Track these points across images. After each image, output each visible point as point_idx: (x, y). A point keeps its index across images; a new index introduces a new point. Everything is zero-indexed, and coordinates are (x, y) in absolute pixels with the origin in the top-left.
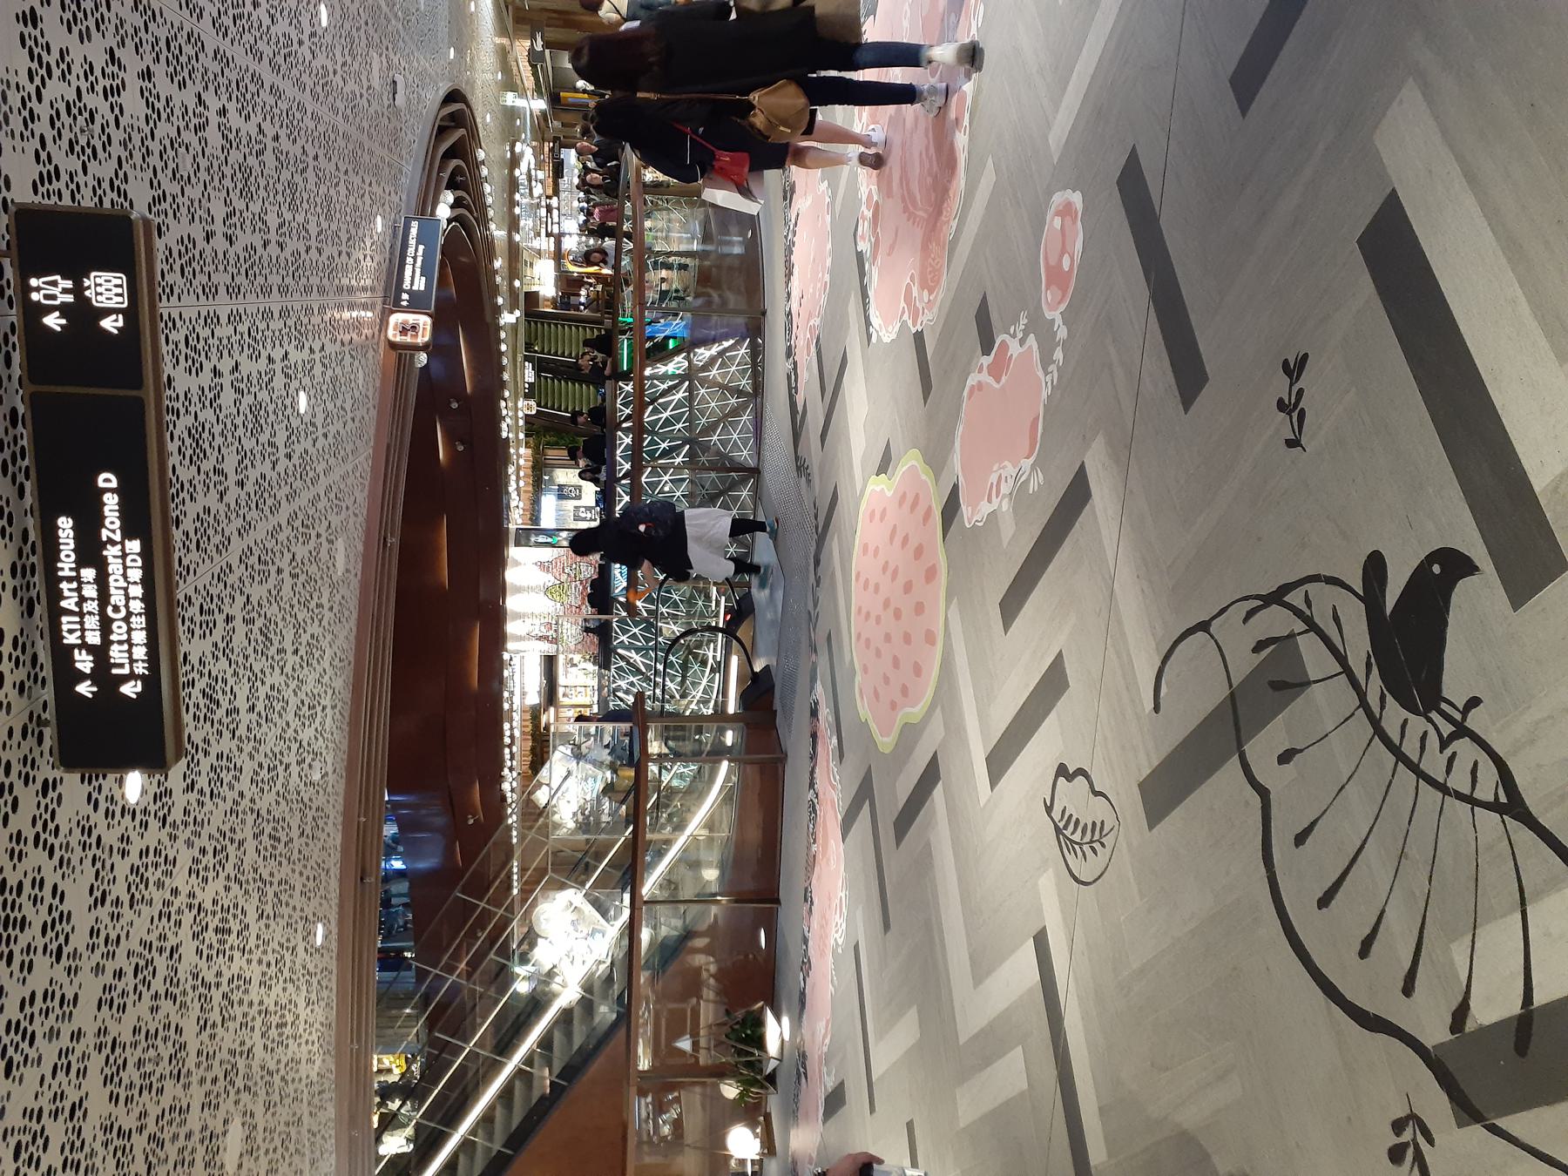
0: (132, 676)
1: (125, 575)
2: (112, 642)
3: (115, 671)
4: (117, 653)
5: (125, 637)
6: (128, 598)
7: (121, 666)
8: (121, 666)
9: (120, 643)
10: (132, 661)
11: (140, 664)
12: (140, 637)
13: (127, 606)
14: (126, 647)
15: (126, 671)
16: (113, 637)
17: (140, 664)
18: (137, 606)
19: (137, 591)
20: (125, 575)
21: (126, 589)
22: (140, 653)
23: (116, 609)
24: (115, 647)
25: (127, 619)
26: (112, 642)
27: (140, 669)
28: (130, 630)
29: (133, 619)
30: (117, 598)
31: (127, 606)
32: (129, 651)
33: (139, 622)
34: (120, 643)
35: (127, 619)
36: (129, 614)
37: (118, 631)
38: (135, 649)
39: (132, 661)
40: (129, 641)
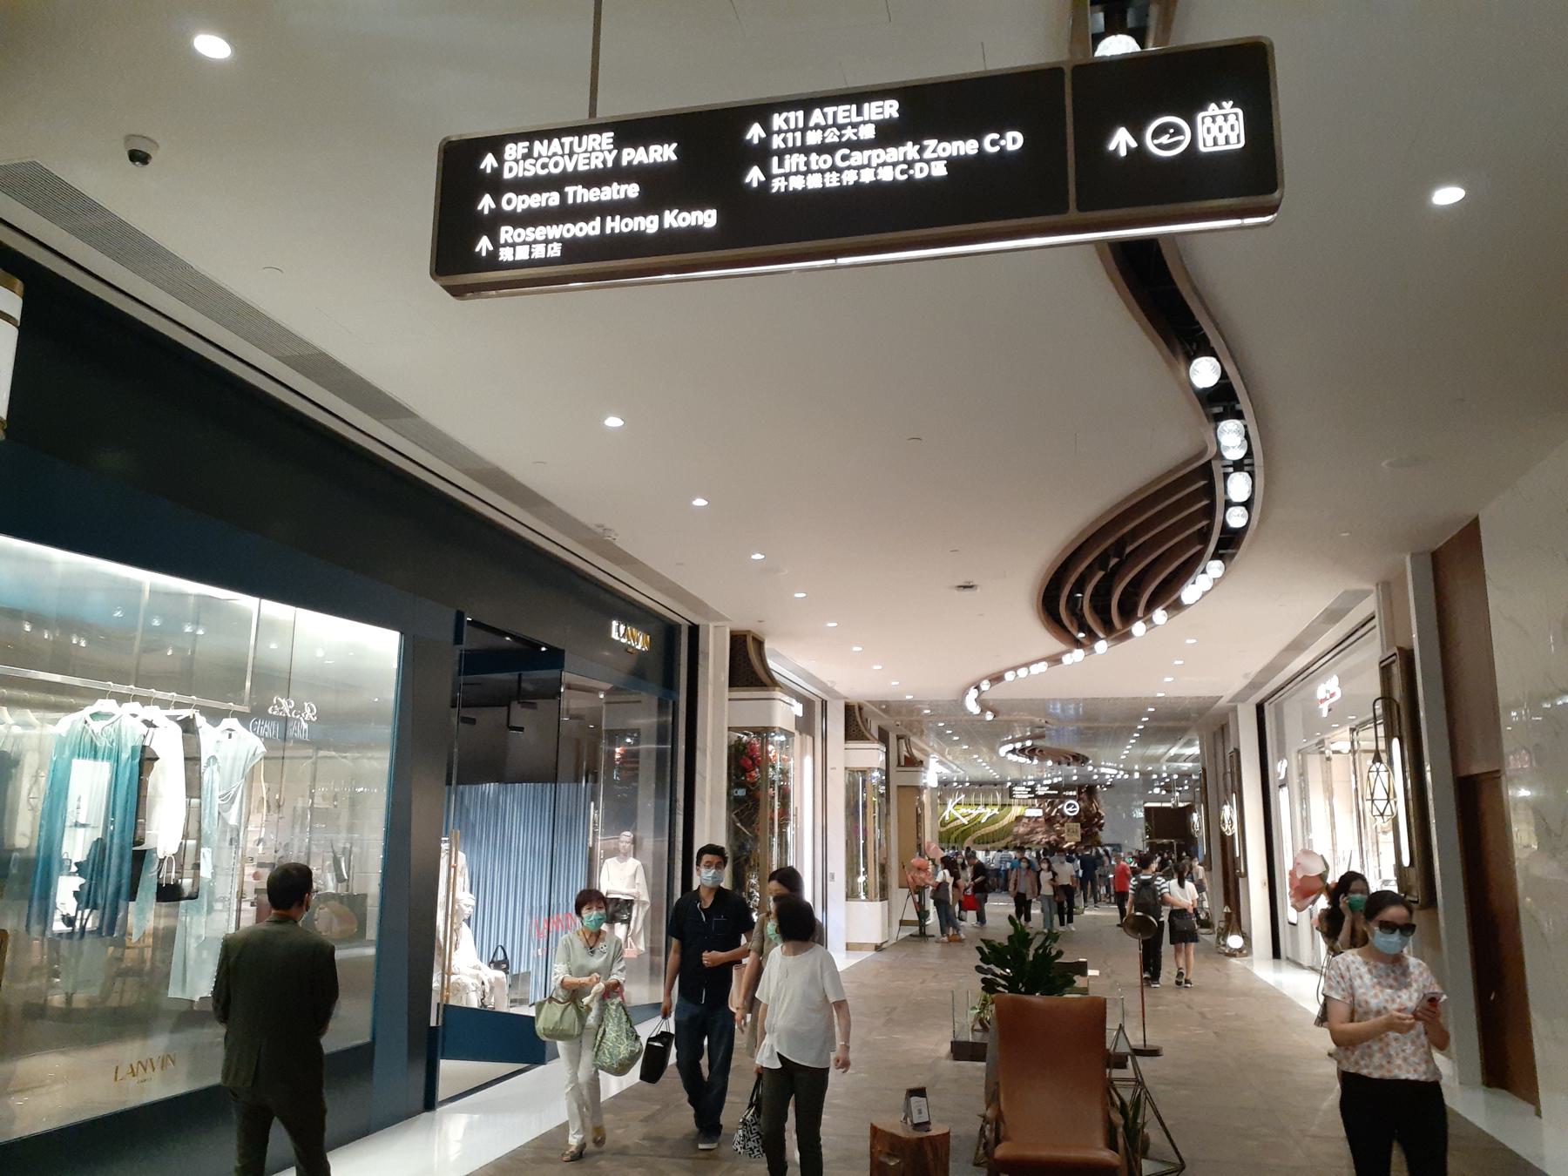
0: (769, 177)
1: (884, 164)
4: (795, 161)
5: (814, 167)
6: (858, 168)
7: (781, 165)
8: (781, 165)
9: (807, 164)
10: (786, 176)
11: (783, 184)
12: (814, 182)
13: (849, 168)
15: (775, 170)
16: (814, 156)
17: (783, 184)
18: (850, 178)
19: (867, 177)
20: (884, 164)
21: (869, 166)
22: (797, 183)
24: (802, 158)
25: (834, 168)
27: (778, 185)
28: (822, 172)
30: (858, 158)
31: (849, 168)
32: (797, 173)
33: (832, 181)
34: (807, 164)
39: (786, 176)
40: (809, 171)
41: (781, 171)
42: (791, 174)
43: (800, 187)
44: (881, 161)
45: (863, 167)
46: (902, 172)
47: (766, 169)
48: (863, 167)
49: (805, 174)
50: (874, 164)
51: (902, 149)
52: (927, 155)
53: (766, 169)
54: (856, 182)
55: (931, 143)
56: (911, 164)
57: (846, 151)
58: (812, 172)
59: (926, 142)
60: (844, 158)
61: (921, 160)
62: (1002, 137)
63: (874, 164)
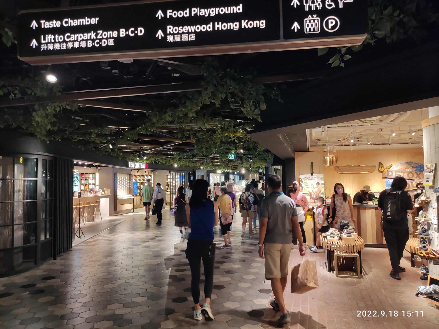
1: (83, 40)
2: (54, 36)
3: (42, 36)
4: (50, 37)
5: (57, 41)
6: (73, 42)
7: (44, 39)
8: (44, 39)
9: (54, 39)
10: (47, 44)
11: (45, 47)
12: (57, 47)
13: (70, 41)
14: (53, 41)
15: (43, 42)
16: (57, 36)
17: (45, 47)
18: (70, 45)
19: (76, 45)
20: (83, 40)
21: (77, 41)
22: (51, 47)
23: (68, 37)
24: (53, 37)
25: (64, 41)
26: (54, 36)
27: (43, 47)
28: (60, 43)
29: (64, 44)
30: (73, 37)
31: (70, 41)
32: (51, 43)
33: (64, 46)
34: (54, 39)
35: (64, 41)
36: (67, 42)
37: (59, 38)
38: (52, 45)
40: (55, 42)
41: (45, 42)
42: (48, 43)
43: (52, 49)
44: (81, 39)
45: (75, 41)
46: (97, 43)
47: (39, 41)
48: (75, 41)
49: (53, 43)
50: (79, 40)
51: (89, 34)
52: (99, 37)
53: (39, 41)
54: (72, 48)
55: (100, 32)
56: (93, 40)
57: (69, 34)
58: (56, 42)
59: (98, 32)
60: (68, 37)
61: (97, 39)
62: (136, 29)
63: (79, 40)
